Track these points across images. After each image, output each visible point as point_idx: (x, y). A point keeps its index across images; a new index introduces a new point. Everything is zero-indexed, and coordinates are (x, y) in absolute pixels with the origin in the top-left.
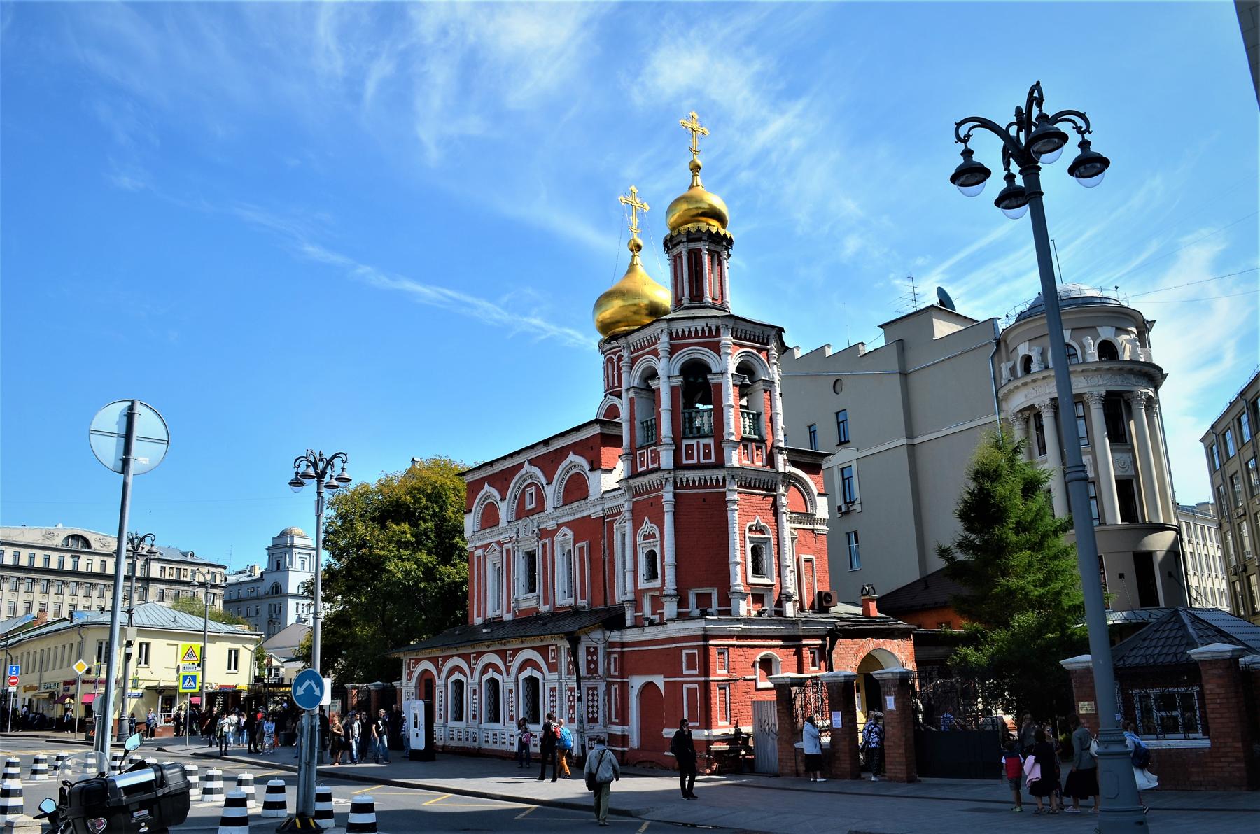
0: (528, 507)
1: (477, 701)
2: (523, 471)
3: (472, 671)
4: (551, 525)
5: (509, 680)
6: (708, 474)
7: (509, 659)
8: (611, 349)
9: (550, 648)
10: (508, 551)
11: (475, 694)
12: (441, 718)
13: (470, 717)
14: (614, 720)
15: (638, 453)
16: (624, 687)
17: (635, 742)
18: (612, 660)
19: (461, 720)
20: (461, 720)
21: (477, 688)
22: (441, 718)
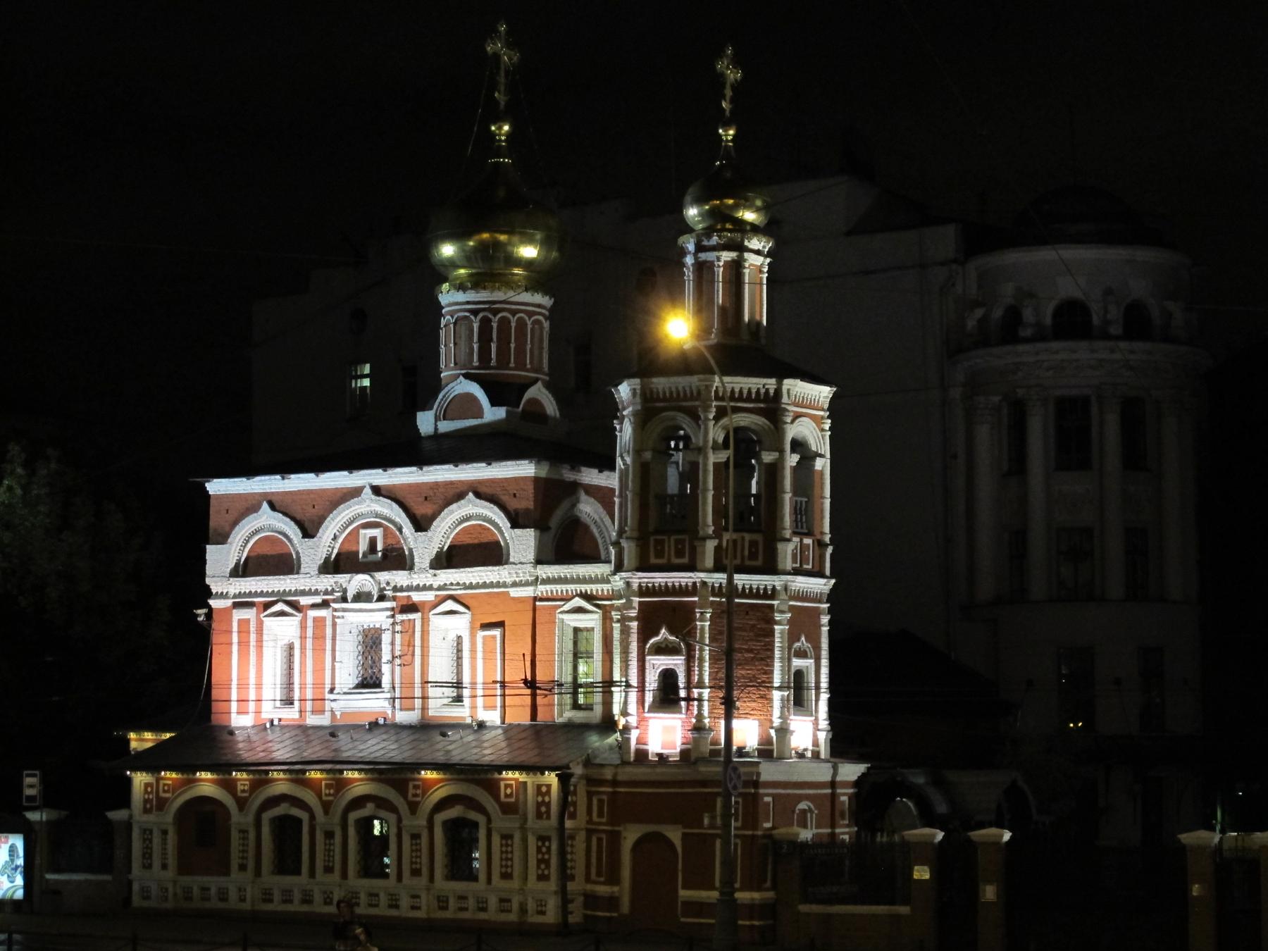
8: (468, 303)
15: (652, 539)
16: (615, 839)
17: (625, 907)
18: (595, 802)
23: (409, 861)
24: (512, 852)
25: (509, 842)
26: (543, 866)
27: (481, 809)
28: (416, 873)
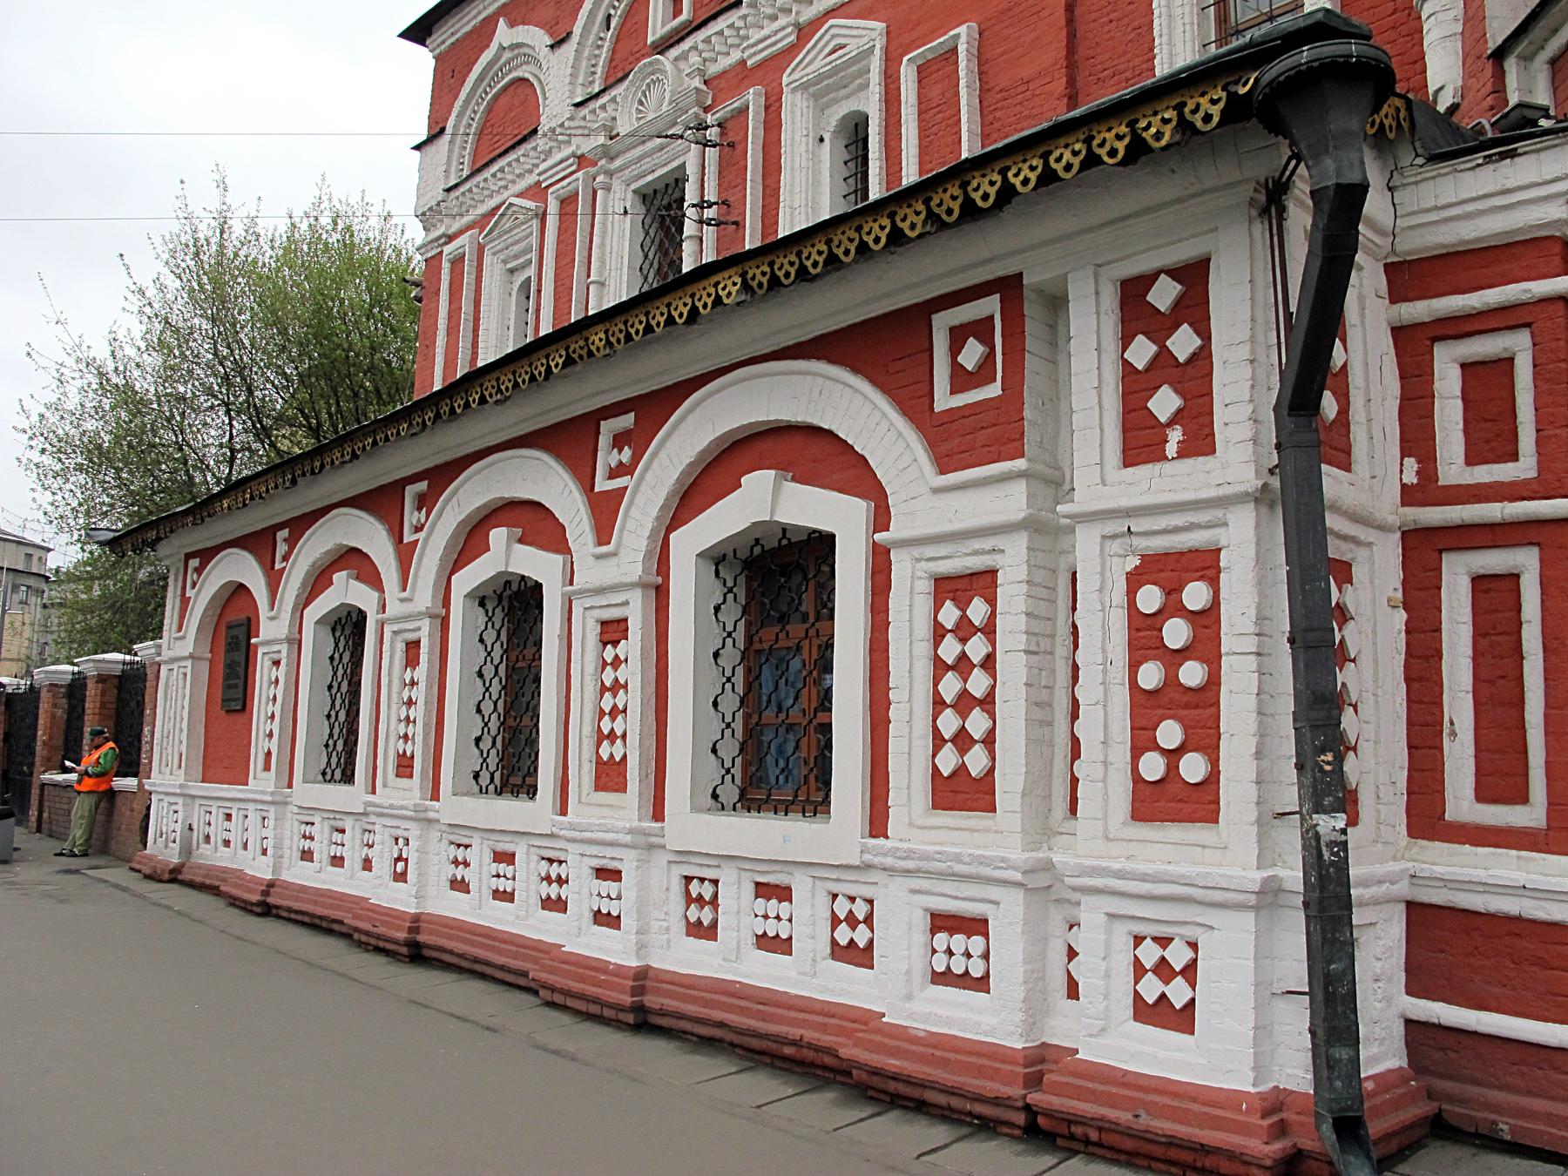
1: (419, 694)
3: (405, 554)
5: (609, 573)
7: (607, 457)
11: (412, 660)
12: (267, 768)
13: (387, 764)
14: (1461, 801)
19: (348, 778)
20: (348, 778)
21: (425, 632)
22: (267, 768)
23: (588, 729)
24: (989, 663)
25: (977, 611)
26: (1170, 733)
28: (610, 776)
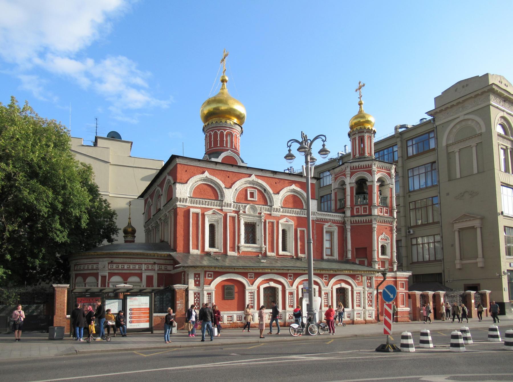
0: (249, 198)
2: (250, 179)
4: (274, 213)
6: (364, 218)
9: (356, 276)
10: (233, 218)
26: (370, 302)
27: (349, 284)
